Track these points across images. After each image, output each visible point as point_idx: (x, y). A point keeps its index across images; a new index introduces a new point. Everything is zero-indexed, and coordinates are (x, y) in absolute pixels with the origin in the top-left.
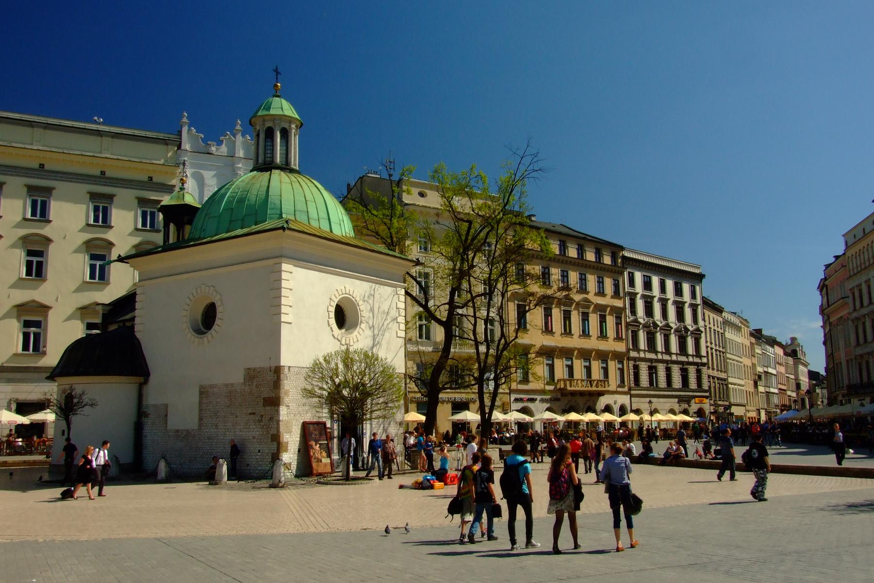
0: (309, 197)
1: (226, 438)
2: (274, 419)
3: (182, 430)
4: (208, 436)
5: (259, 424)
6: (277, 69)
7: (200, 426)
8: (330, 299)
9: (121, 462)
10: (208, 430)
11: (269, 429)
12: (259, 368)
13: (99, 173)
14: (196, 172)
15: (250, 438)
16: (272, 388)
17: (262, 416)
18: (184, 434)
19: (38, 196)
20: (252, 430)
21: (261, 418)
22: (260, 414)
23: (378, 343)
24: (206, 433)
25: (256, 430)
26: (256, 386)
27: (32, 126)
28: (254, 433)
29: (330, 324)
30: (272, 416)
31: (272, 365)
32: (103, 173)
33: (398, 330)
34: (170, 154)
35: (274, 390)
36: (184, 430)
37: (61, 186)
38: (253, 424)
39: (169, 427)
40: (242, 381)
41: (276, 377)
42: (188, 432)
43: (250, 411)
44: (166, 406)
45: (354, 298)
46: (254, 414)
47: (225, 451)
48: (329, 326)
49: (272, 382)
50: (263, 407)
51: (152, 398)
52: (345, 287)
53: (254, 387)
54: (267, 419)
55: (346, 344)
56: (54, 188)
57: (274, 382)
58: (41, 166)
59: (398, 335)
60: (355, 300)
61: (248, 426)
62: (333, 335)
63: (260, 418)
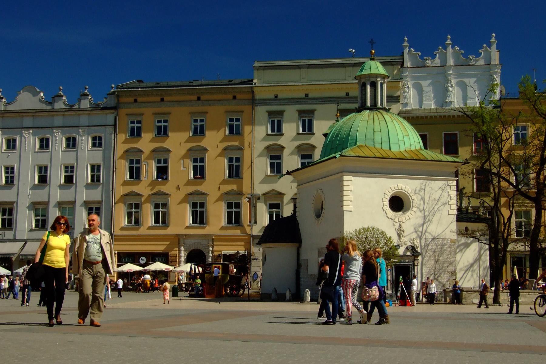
0: (377, 128)
6: (372, 40)
8: (385, 194)
9: (278, 293)
13: (344, 95)
14: (415, 82)
19: (305, 117)
23: (429, 221)
27: (300, 68)
29: (384, 210)
32: (348, 94)
33: (450, 210)
34: (395, 72)
37: (320, 108)
39: (308, 273)
44: (307, 260)
45: (406, 191)
48: (384, 211)
51: (303, 257)
52: (398, 185)
55: (399, 222)
56: (315, 110)
58: (307, 96)
59: (450, 213)
60: (407, 193)
62: (387, 216)
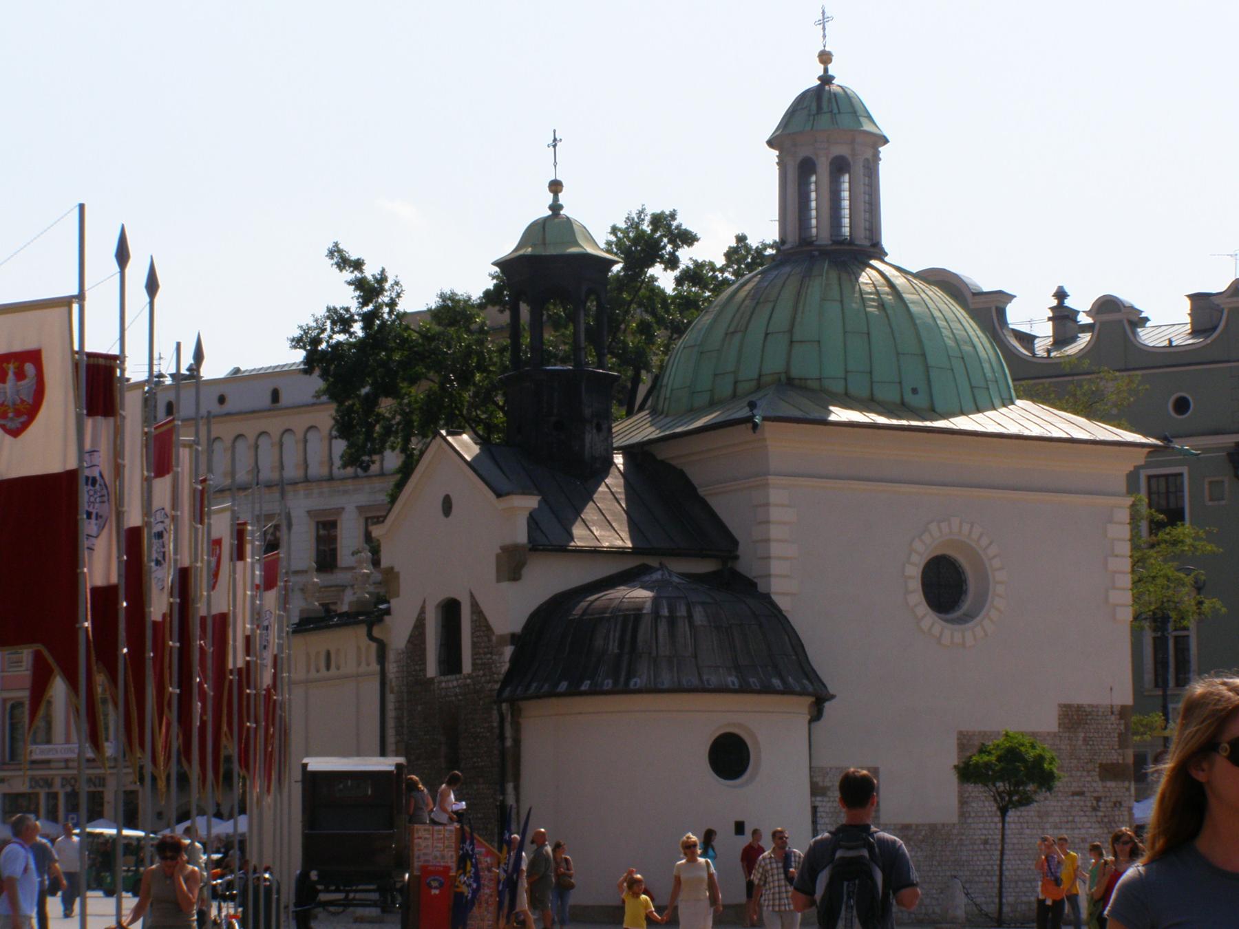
1: (1023, 841)
2: (1123, 803)
3: (917, 826)
4: (983, 837)
5: (1094, 814)
7: (963, 815)
10: (981, 825)
11: (1113, 825)
12: (1089, 705)
15: (1077, 841)
16: (1116, 747)
17: (1098, 799)
18: (923, 833)
20: (1079, 826)
21: (1097, 803)
22: (1096, 794)
24: (979, 832)
25: (1088, 825)
26: (1084, 740)
28: (1083, 831)
30: (1119, 799)
31: (1114, 704)
35: (1119, 751)
36: (924, 825)
38: (1082, 813)
40: (1056, 730)
41: (1122, 727)
42: (933, 828)
43: (1073, 789)
46: (1081, 794)
47: (1022, 867)
49: (1116, 735)
50: (1100, 783)
53: (1080, 742)
54: (1108, 805)
57: (1120, 735)
61: (1070, 818)
63: (1095, 802)
